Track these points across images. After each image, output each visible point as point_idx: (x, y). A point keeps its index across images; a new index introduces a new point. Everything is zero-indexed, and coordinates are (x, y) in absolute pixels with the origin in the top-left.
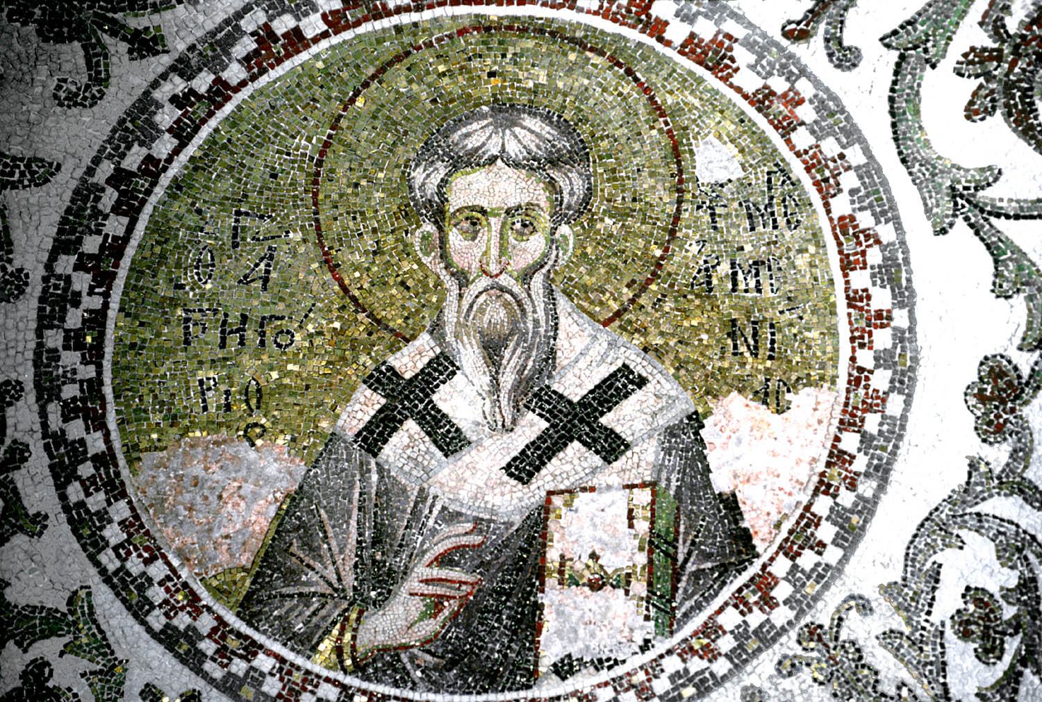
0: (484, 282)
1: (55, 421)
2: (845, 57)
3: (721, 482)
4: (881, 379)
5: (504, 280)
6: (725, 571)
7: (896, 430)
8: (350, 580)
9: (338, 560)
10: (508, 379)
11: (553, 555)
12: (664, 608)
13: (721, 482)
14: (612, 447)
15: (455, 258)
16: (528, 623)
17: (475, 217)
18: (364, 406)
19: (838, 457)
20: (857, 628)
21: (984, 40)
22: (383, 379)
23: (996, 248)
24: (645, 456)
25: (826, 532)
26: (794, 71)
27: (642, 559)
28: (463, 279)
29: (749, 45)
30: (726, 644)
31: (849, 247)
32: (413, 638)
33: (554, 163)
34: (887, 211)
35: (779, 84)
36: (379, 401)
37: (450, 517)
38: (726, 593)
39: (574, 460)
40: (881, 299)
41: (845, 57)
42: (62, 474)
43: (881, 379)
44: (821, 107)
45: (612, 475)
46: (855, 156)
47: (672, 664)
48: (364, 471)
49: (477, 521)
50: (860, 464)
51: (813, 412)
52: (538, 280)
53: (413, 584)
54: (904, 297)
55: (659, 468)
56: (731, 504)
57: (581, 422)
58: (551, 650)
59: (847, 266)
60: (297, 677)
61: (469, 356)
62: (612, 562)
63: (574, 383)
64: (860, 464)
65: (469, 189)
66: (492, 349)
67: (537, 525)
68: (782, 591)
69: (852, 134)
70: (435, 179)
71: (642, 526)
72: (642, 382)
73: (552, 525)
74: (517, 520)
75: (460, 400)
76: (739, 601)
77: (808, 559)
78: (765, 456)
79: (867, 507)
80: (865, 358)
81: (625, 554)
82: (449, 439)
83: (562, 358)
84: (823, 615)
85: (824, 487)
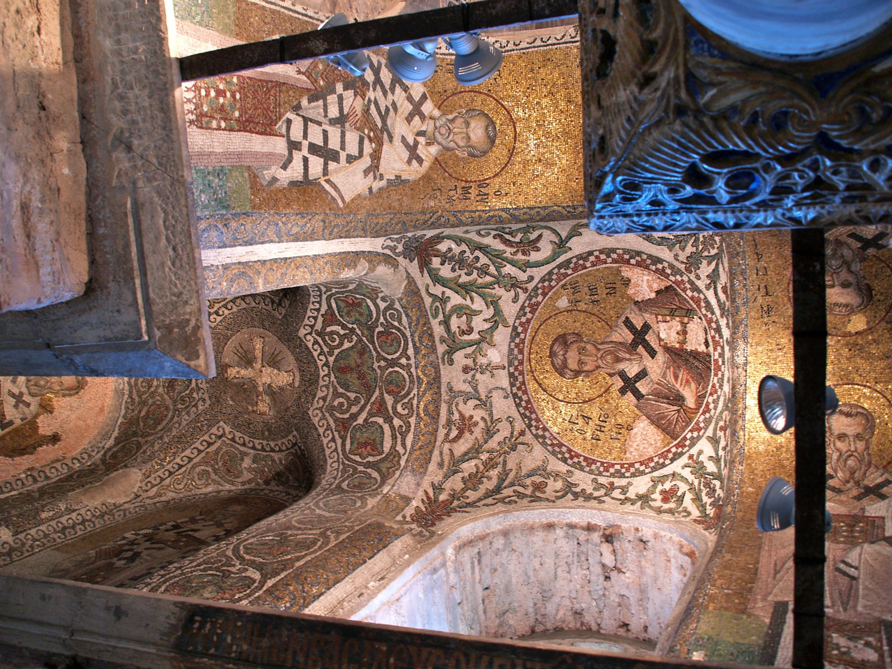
0: (599, 361)
1: (608, 474)
2: (531, 278)
3: (653, 295)
4: (615, 256)
5: (599, 355)
6: (678, 295)
7: (626, 251)
8: (676, 408)
9: (670, 410)
10: (627, 356)
11: (677, 346)
12: (689, 313)
13: (653, 295)
14: (646, 327)
15: (591, 369)
16: (695, 354)
17: (581, 363)
18: (630, 396)
19: (638, 264)
20: (683, 257)
21: (520, 253)
22: (623, 391)
23: (569, 238)
24: (649, 318)
25: (660, 266)
26: (536, 288)
27: (677, 319)
28: (598, 367)
29: (530, 300)
30: (696, 294)
31: (580, 268)
32: (694, 390)
33: (566, 343)
34: (569, 261)
35: (540, 291)
36: (629, 393)
37: (664, 376)
38: (683, 294)
39: (650, 337)
40: (592, 258)
41: (531, 278)
42: (622, 476)
43: (615, 256)
44: (545, 281)
45: (654, 326)
46: (556, 271)
47: (704, 312)
48: (648, 399)
49: (667, 368)
50: (638, 259)
51: (626, 272)
52: (599, 347)
53: (681, 390)
54: (590, 253)
55: (651, 314)
56: (658, 292)
57: (640, 336)
58: (702, 348)
59: (586, 268)
60: (696, 426)
61: (621, 366)
62: (679, 328)
63: (630, 337)
64: (638, 259)
65: (573, 364)
66: (618, 360)
67: (668, 349)
68: (679, 278)
69: (550, 273)
70: (569, 372)
71: (668, 318)
72: (627, 318)
73: (669, 345)
74: (667, 355)
75: (632, 370)
76: (684, 290)
77: (669, 271)
78: (644, 285)
79: (650, 256)
80: (609, 260)
81: (676, 325)
82: (642, 374)
83: (622, 340)
84: (682, 267)
85: (647, 267)
